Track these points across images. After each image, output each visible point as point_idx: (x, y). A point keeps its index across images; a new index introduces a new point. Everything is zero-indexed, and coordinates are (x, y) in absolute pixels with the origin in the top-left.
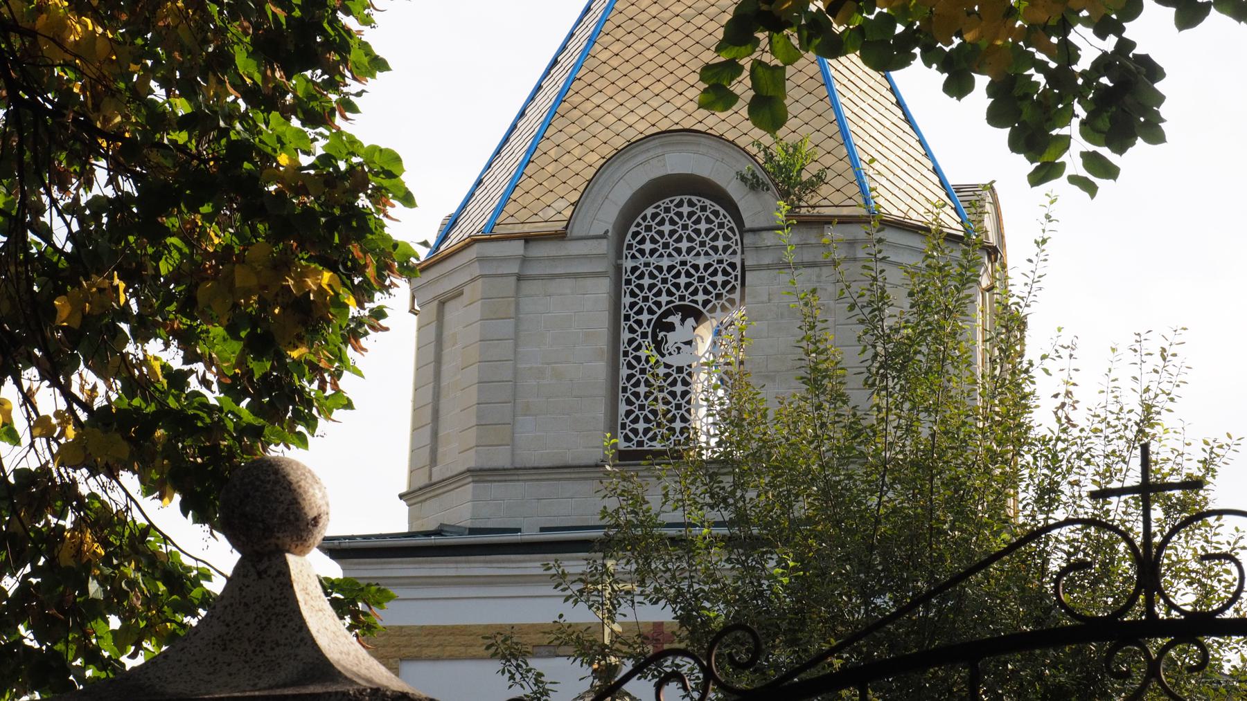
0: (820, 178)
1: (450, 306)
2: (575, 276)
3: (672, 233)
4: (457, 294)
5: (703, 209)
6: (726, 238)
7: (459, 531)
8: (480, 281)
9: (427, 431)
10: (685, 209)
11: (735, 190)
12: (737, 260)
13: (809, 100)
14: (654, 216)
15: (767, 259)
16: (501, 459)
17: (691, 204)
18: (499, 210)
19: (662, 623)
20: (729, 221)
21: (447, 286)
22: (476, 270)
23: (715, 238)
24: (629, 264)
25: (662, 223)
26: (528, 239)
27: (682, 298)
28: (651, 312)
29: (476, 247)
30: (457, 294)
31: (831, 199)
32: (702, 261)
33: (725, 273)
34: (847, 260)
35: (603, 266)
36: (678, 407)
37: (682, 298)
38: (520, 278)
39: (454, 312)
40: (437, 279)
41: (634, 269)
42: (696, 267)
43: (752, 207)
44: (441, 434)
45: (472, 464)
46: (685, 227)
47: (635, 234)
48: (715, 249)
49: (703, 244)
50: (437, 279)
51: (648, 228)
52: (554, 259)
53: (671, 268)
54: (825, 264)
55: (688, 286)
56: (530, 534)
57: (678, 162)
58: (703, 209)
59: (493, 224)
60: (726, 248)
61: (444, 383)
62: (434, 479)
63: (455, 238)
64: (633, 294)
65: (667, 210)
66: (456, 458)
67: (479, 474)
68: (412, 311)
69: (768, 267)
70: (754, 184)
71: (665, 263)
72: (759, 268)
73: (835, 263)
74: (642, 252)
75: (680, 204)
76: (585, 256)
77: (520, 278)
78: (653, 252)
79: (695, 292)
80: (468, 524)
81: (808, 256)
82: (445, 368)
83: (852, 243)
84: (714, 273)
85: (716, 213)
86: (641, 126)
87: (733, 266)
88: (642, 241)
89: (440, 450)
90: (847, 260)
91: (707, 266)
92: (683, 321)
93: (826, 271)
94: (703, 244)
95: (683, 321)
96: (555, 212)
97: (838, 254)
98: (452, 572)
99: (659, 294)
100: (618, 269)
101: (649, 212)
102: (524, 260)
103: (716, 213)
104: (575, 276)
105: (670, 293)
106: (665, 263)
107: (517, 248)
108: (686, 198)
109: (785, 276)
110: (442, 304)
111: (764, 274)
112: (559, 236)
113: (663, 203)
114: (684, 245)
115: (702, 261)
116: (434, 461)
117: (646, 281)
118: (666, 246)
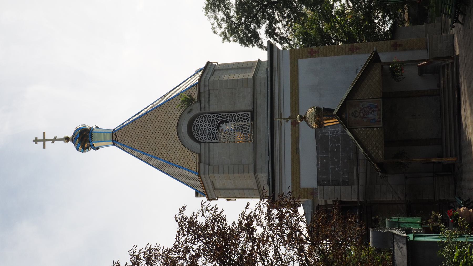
0: (190, 96)
1: (216, 187)
2: (209, 152)
3: (201, 131)
4: (212, 182)
5: (195, 124)
6: (202, 118)
7: (269, 179)
8: (210, 175)
9: (245, 191)
10: (195, 128)
11: (191, 115)
12: (208, 115)
13: (173, 103)
14: (197, 135)
15: (207, 106)
16: (251, 167)
17: (194, 127)
18: (193, 172)
19: (291, 123)
20: (199, 118)
21: (211, 186)
22: (207, 176)
23: (202, 120)
24: (207, 141)
25: (198, 133)
26: (200, 162)
27: (216, 127)
28: (217, 122)
29: (201, 175)
30: (212, 182)
31: (195, 96)
32: (208, 123)
33: (210, 118)
34: (208, 87)
35: (207, 144)
36: (241, 127)
37: (216, 127)
38: (209, 165)
39: (218, 185)
40: (209, 189)
41: (209, 139)
42: (209, 124)
43: (196, 109)
44: (246, 187)
45: (253, 174)
46: (199, 128)
47: (201, 139)
48: (205, 120)
49: (204, 123)
50: (209, 189)
51: (199, 136)
52: (205, 157)
53: (209, 131)
54: (209, 92)
55: (213, 126)
56: (269, 158)
57: (184, 129)
58: (195, 124)
59: (196, 173)
60: (205, 118)
61: (234, 187)
62: (256, 188)
63: (201, 191)
64: (214, 139)
65: (195, 132)
66: (251, 183)
67: (255, 172)
68: (217, 200)
69: (209, 105)
70: (191, 110)
71: (207, 132)
72: (209, 108)
73: (209, 90)
74: (205, 138)
75: (194, 129)
76: (205, 149)
77: (209, 165)
78: (205, 135)
79: (215, 124)
80: (267, 174)
81: (207, 96)
82: (230, 187)
83: (205, 86)
84: (210, 120)
85: (197, 121)
86: (174, 133)
87: (209, 116)
88: (202, 138)
89: (250, 187)
90: (208, 87)
91: (209, 122)
92: (221, 127)
93: (211, 92)
94: (204, 123)
95: (221, 127)
96: (195, 158)
97: (207, 89)
98: (278, 174)
99: (214, 133)
100: (208, 143)
101: (195, 136)
102: (205, 163)
103: (197, 121)
104: (209, 152)
105: (214, 130)
106: (207, 132)
107: (202, 165)
108: (193, 128)
109: (211, 102)
110: (215, 189)
111: (211, 106)
112: (200, 155)
113: (194, 133)
114: (204, 128)
115: (208, 123)
116: (253, 189)
117: (212, 136)
118: (204, 132)
